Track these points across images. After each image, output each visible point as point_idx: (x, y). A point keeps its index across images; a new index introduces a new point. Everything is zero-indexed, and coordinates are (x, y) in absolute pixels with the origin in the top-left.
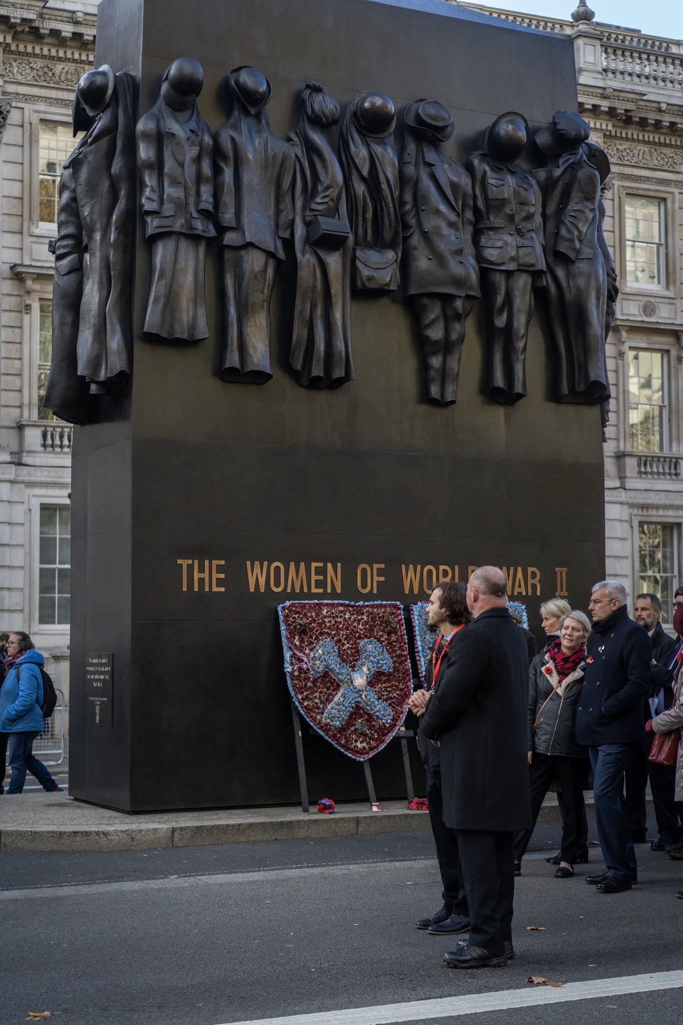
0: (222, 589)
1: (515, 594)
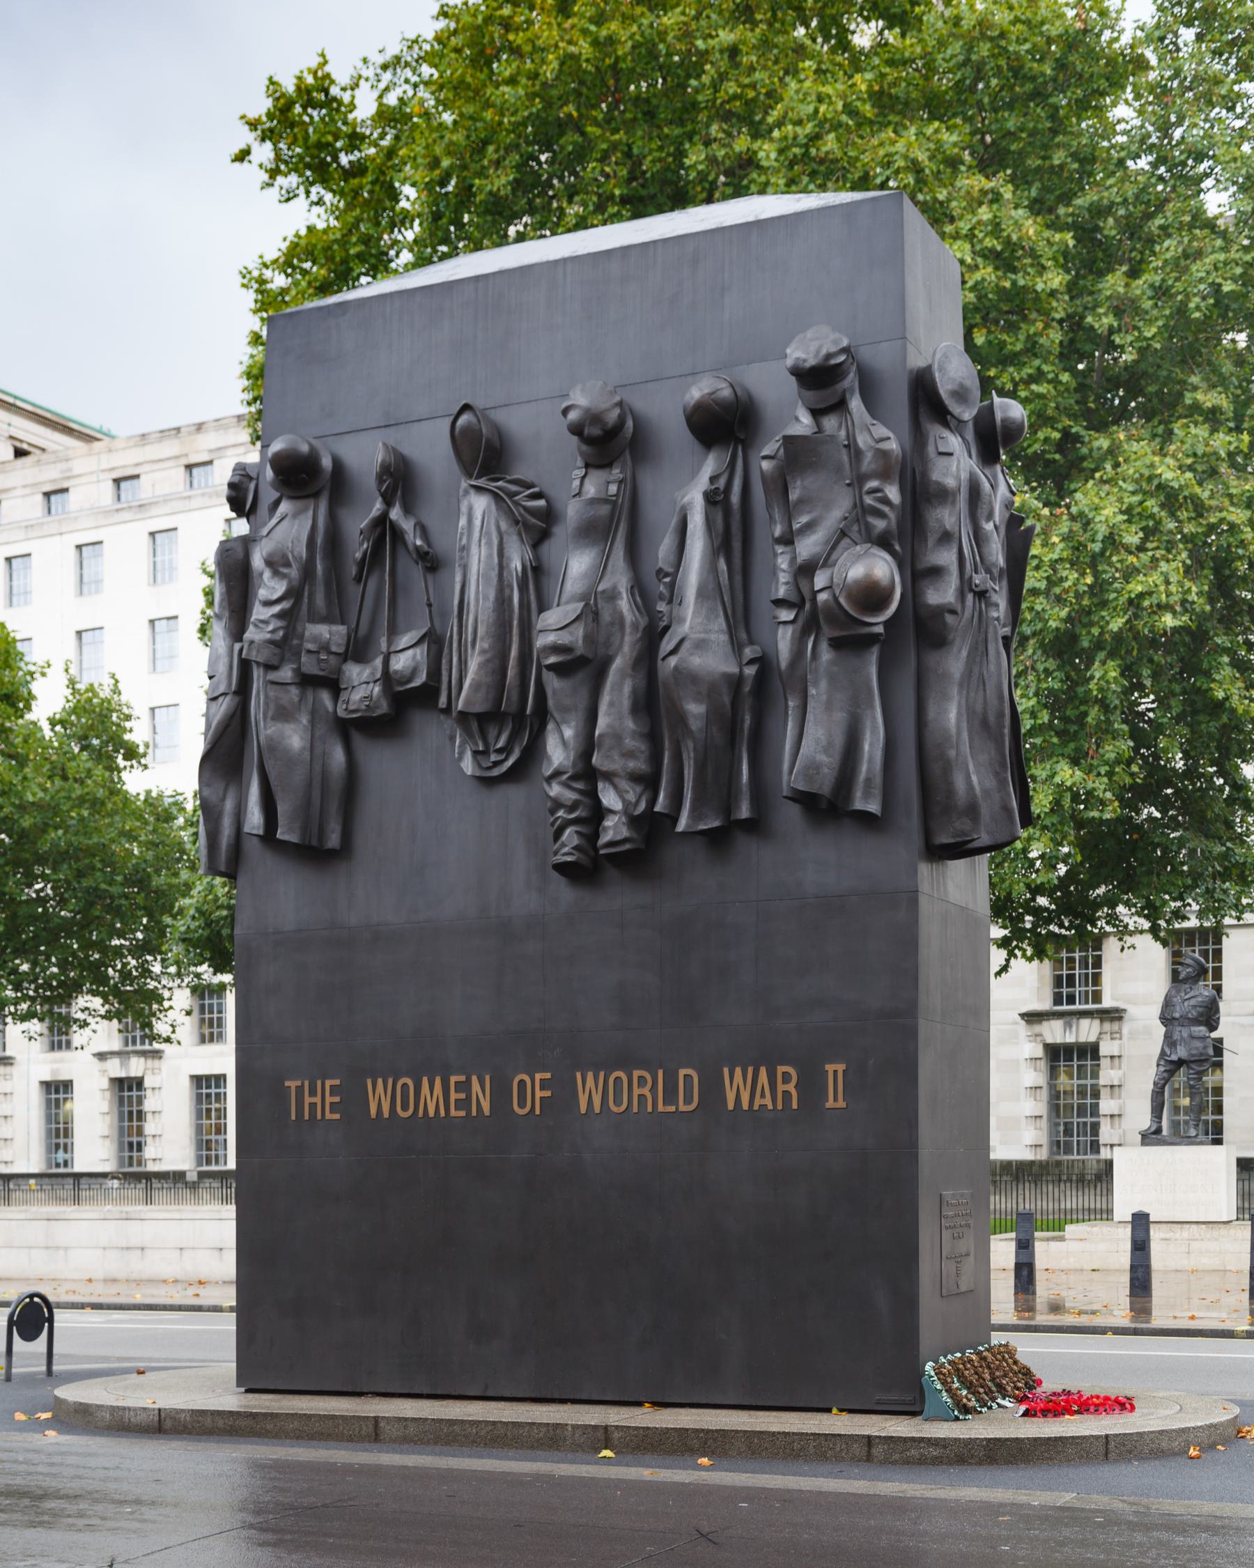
0: (337, 1116)
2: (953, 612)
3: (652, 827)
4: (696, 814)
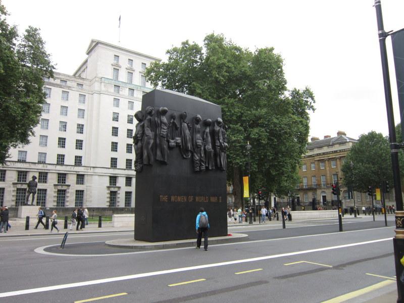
3: (207, 168)
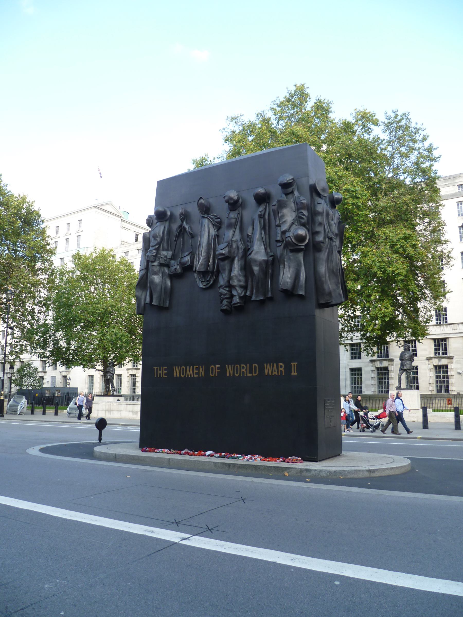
0: (166, 376)
1: (273, 374)
2: (323, 243)
3: (245, 299)
4: (257, 296)
